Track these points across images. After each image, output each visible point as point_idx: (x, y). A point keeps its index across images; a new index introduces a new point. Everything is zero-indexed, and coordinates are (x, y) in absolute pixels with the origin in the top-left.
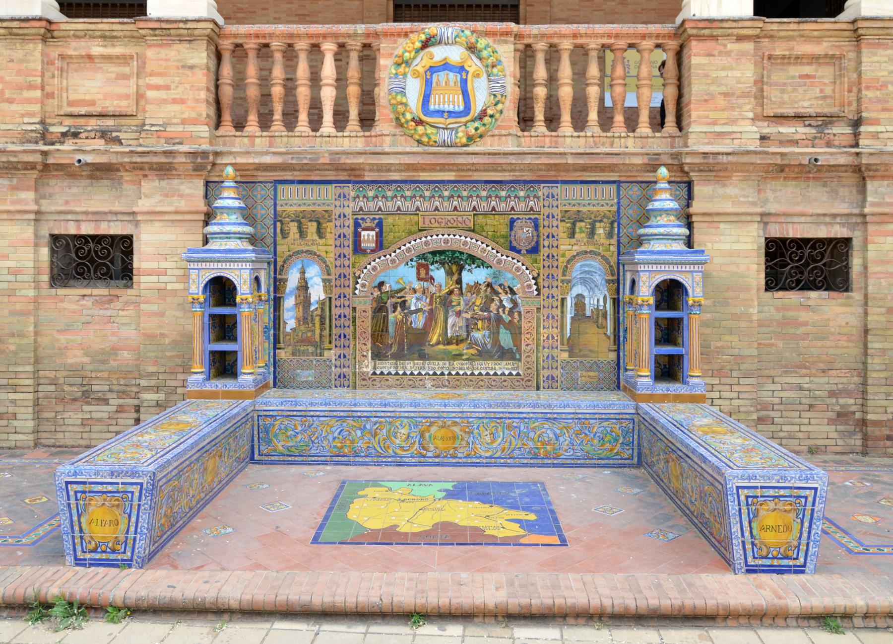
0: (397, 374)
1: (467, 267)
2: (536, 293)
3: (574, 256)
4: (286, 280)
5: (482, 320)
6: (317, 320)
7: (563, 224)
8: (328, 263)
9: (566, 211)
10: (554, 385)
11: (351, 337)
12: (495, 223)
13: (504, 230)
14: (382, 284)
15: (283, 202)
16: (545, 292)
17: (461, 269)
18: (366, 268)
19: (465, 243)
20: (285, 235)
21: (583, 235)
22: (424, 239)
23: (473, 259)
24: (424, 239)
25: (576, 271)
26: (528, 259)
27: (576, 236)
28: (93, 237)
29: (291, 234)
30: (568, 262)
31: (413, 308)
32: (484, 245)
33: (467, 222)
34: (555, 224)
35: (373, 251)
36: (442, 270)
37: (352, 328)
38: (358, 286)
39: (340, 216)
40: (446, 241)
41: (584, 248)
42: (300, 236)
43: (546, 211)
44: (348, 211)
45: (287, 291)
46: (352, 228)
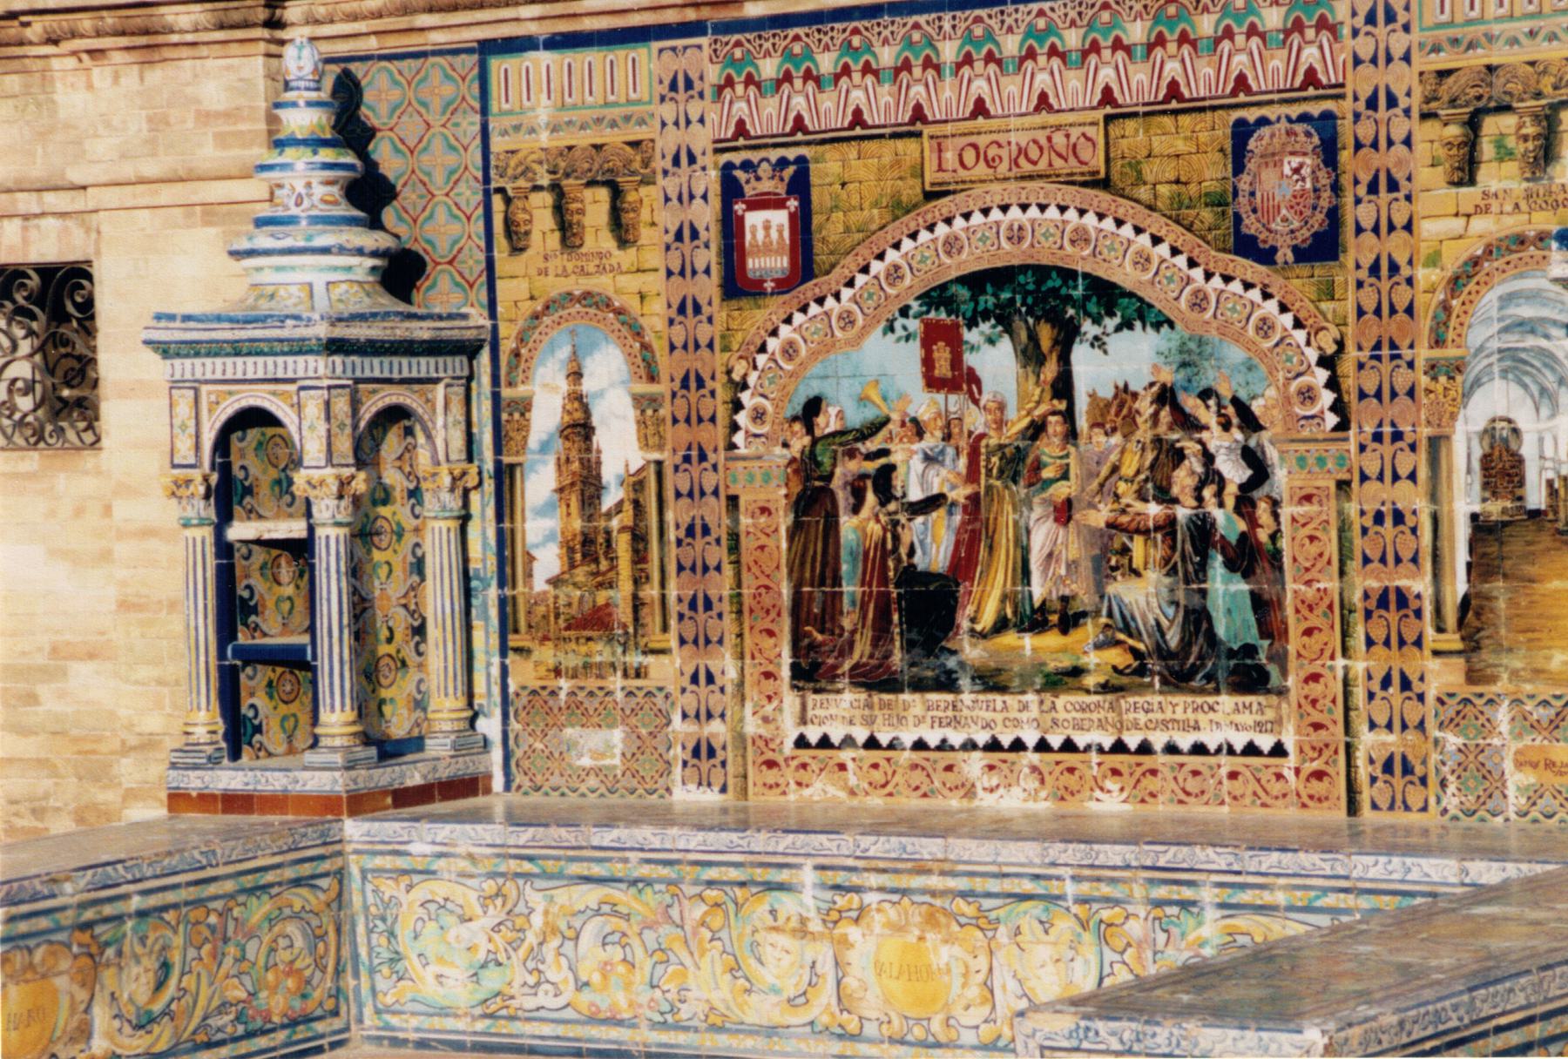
0: (872, 744)
1: (1088, 328)
2: (1332, 420)
3: (1475, 262)
4: (525, 406)
5: (1146, 532)
6: (623, 544)
7: (1432, 127)
8: (649, 337)
9: (1443, 74)
10: (1415, 796)
11: (726, 607)
12: (1181, 146)
13: (1212, 171)
14: (813, 407)
15: (508, 122)
16: (1365, 419)
17: (1067, 336)
18: (763, 349)
19: (1080, 237)
20: (517, 240)
21: (1512, 167)
22: (942, 229)
23: (1106, 295)
24: (942, 229)
25: (1482, 329)
26: (1300, 284)
27: (1483, 174)
29: (536, 237)
30: (1455, 283)
31: (915, 495)
32: (1144, 240)
33: (1085, 152)
34: (1399, 130)
35: (785, 285)
36: (1005, 344)
37: (728, 570)
38: (742, 418)
39: (676, 161)
40: (1017, 235)
41: (1513, 224)
42: (563, 240)
43: (1363, 82)
44: (701, 139)
45: (534, 441)
46: (716, 201)
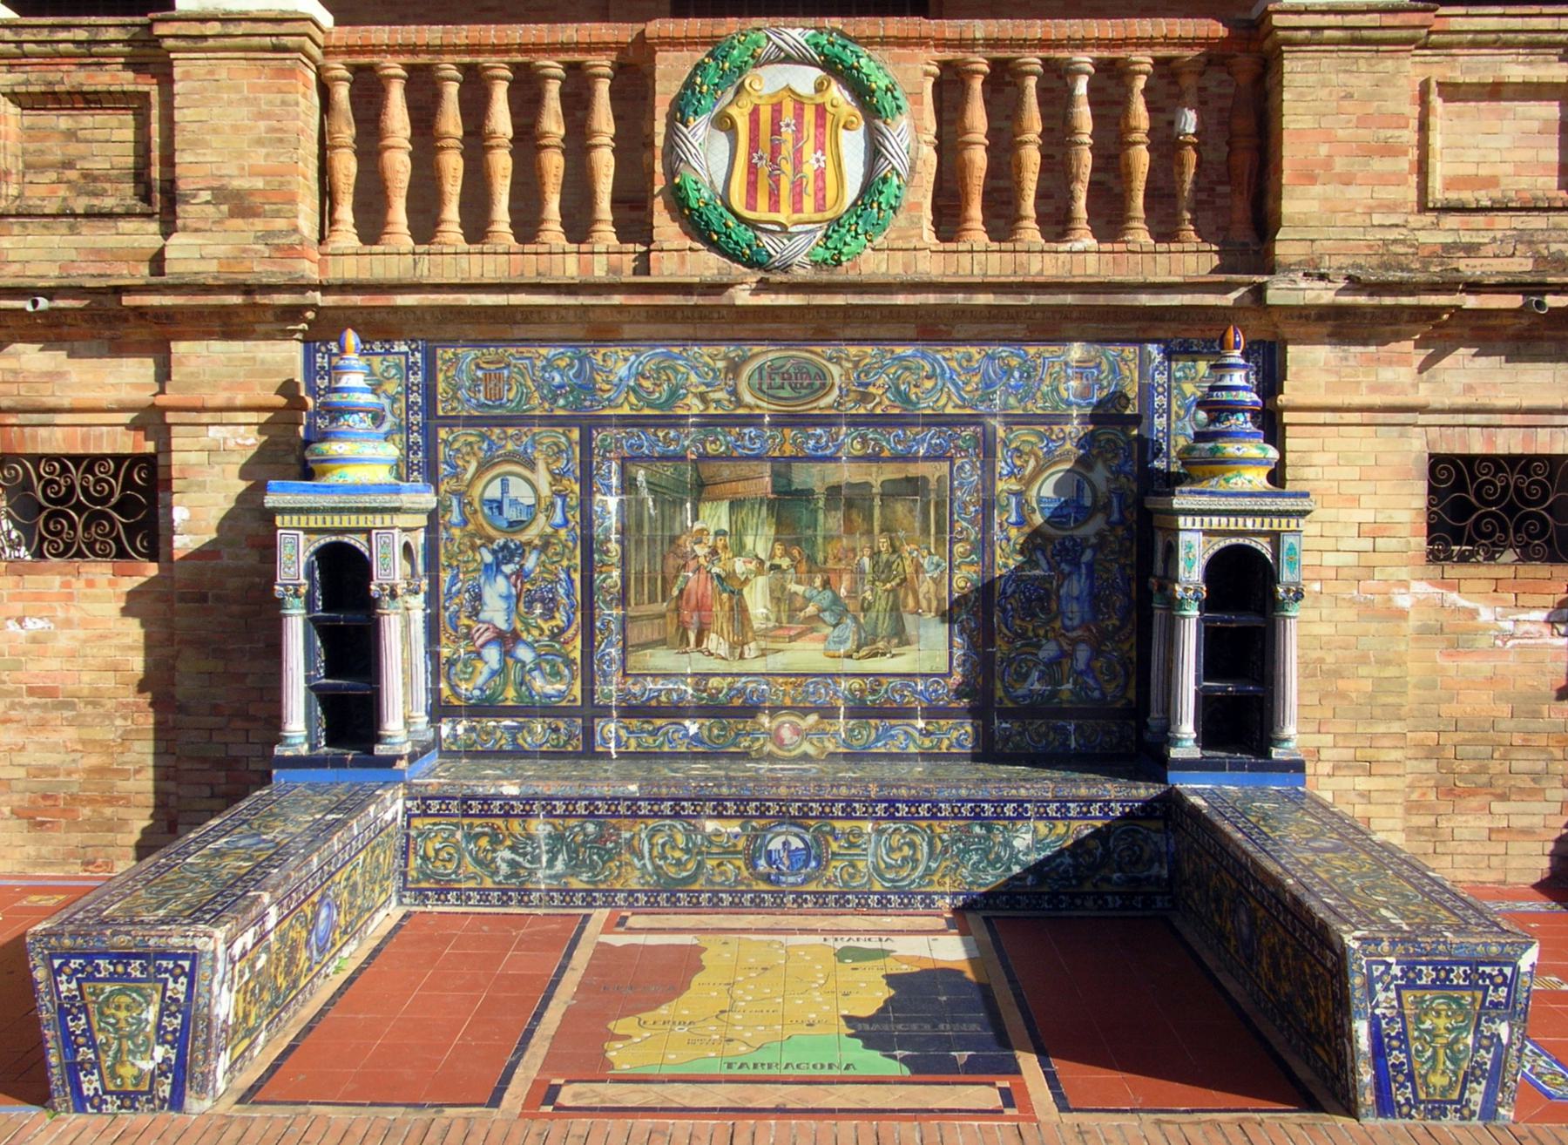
28: (1512, 459)
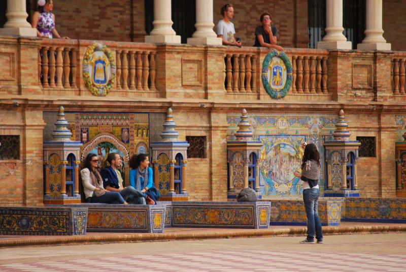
17: (109, 149)
26: (126, 145)
